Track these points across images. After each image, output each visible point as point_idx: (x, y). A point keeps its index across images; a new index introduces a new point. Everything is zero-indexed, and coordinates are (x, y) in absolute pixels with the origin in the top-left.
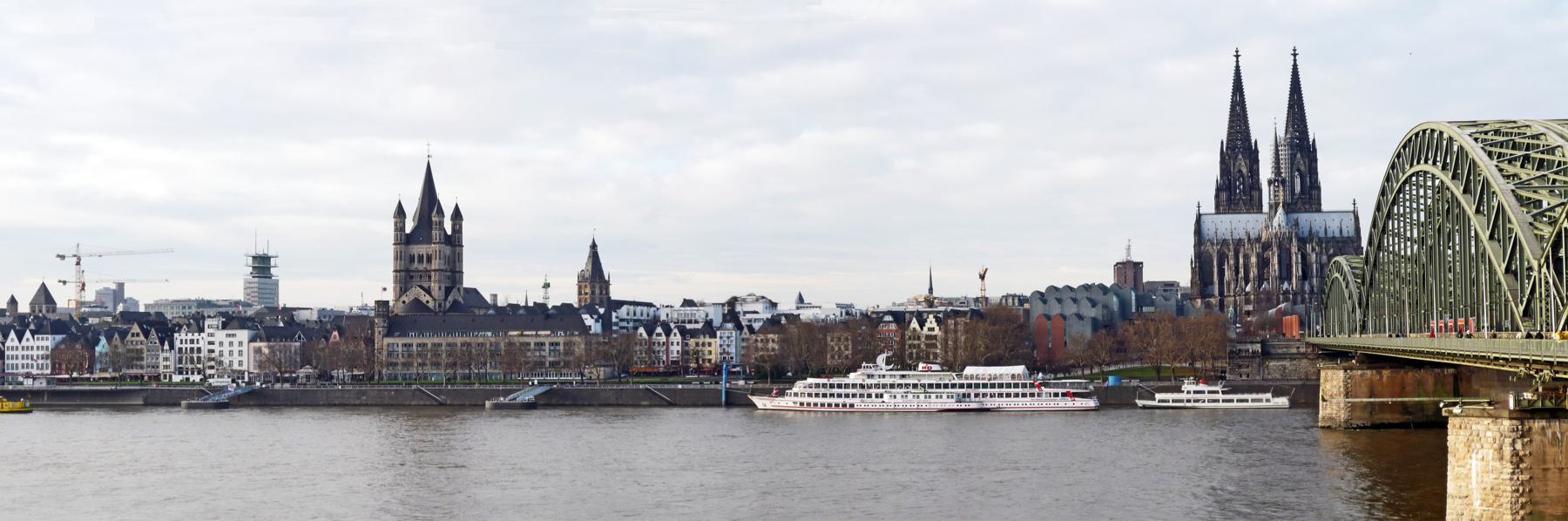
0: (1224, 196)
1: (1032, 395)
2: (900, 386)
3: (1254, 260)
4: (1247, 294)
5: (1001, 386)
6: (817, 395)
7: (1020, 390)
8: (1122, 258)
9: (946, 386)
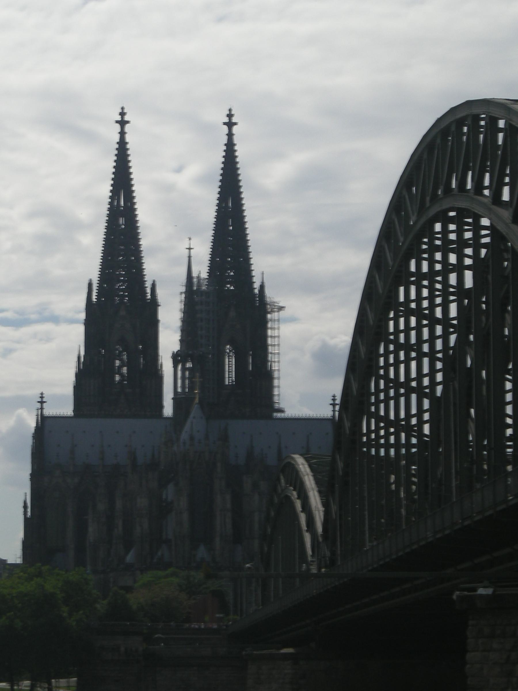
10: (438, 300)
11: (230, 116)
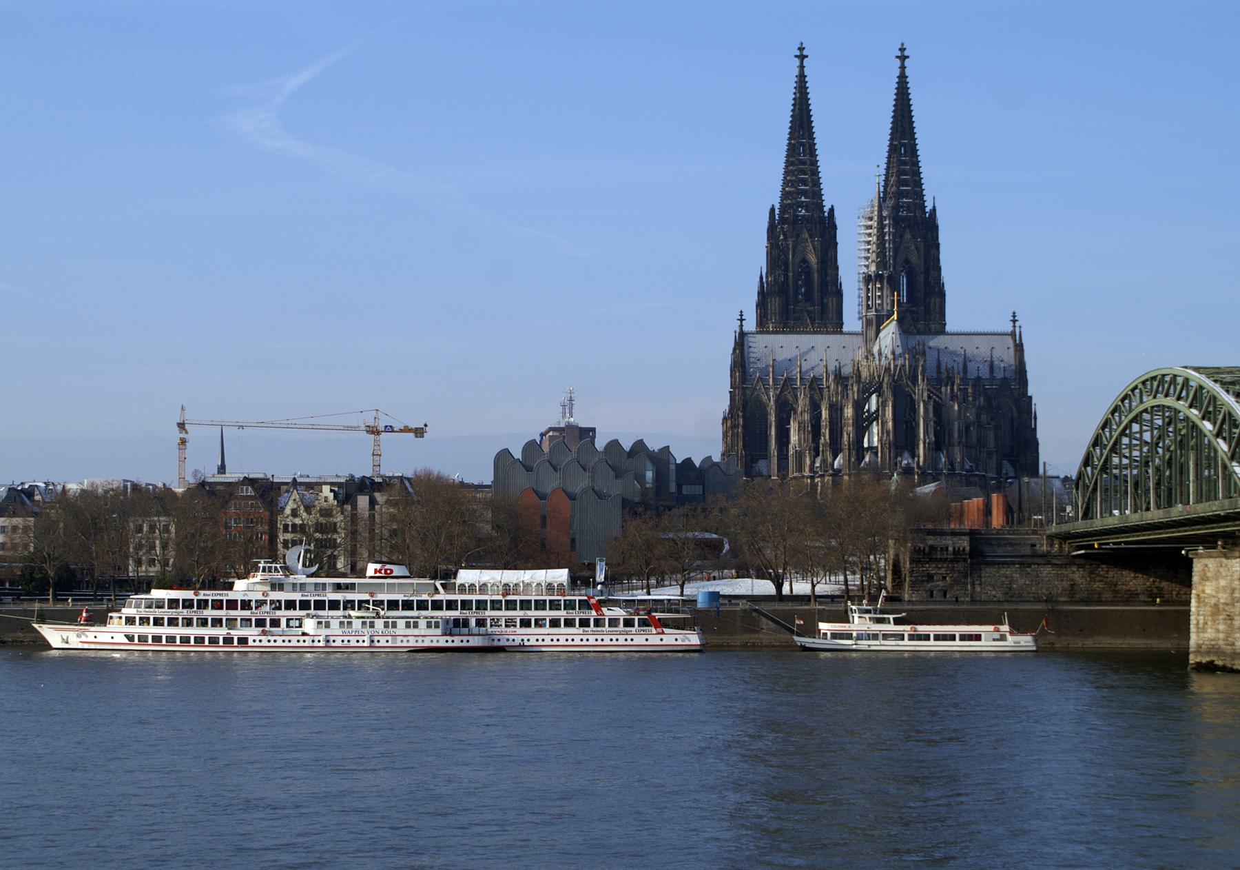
1: (584, 623)
2: (334, 605)
3: (849, 412)
4: (837, 473)
5: (525, 605)
6: (173, 622)
7: (561, 614)
9: (422, 605)
11: (902, 50)
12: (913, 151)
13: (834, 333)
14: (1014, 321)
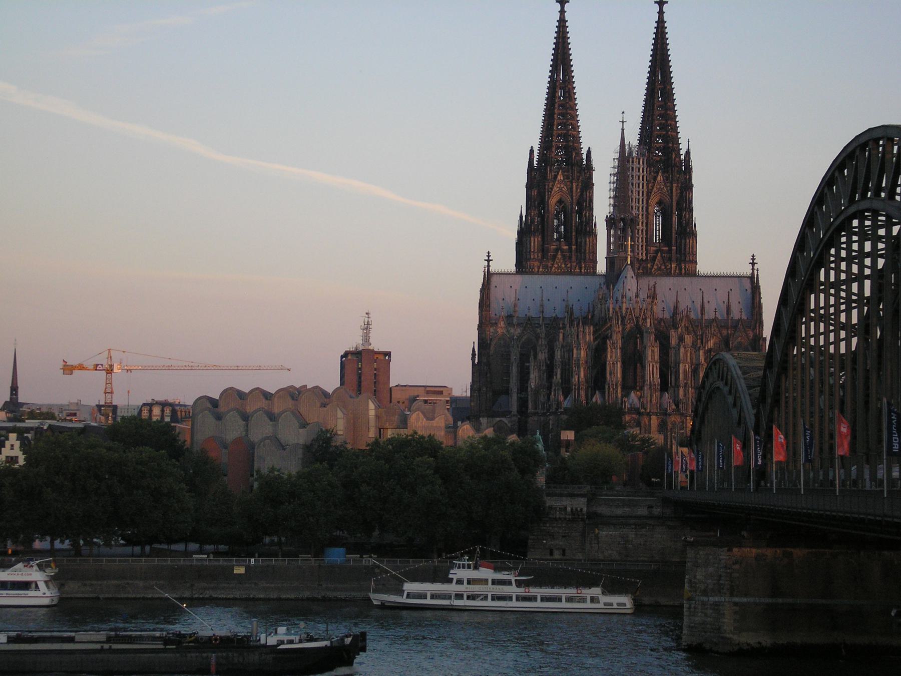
0: (535, 242)
8: (354, 341)
10: (843, 307)
12: (668, 95)
13: (587, 274)
14: (753, 264)
